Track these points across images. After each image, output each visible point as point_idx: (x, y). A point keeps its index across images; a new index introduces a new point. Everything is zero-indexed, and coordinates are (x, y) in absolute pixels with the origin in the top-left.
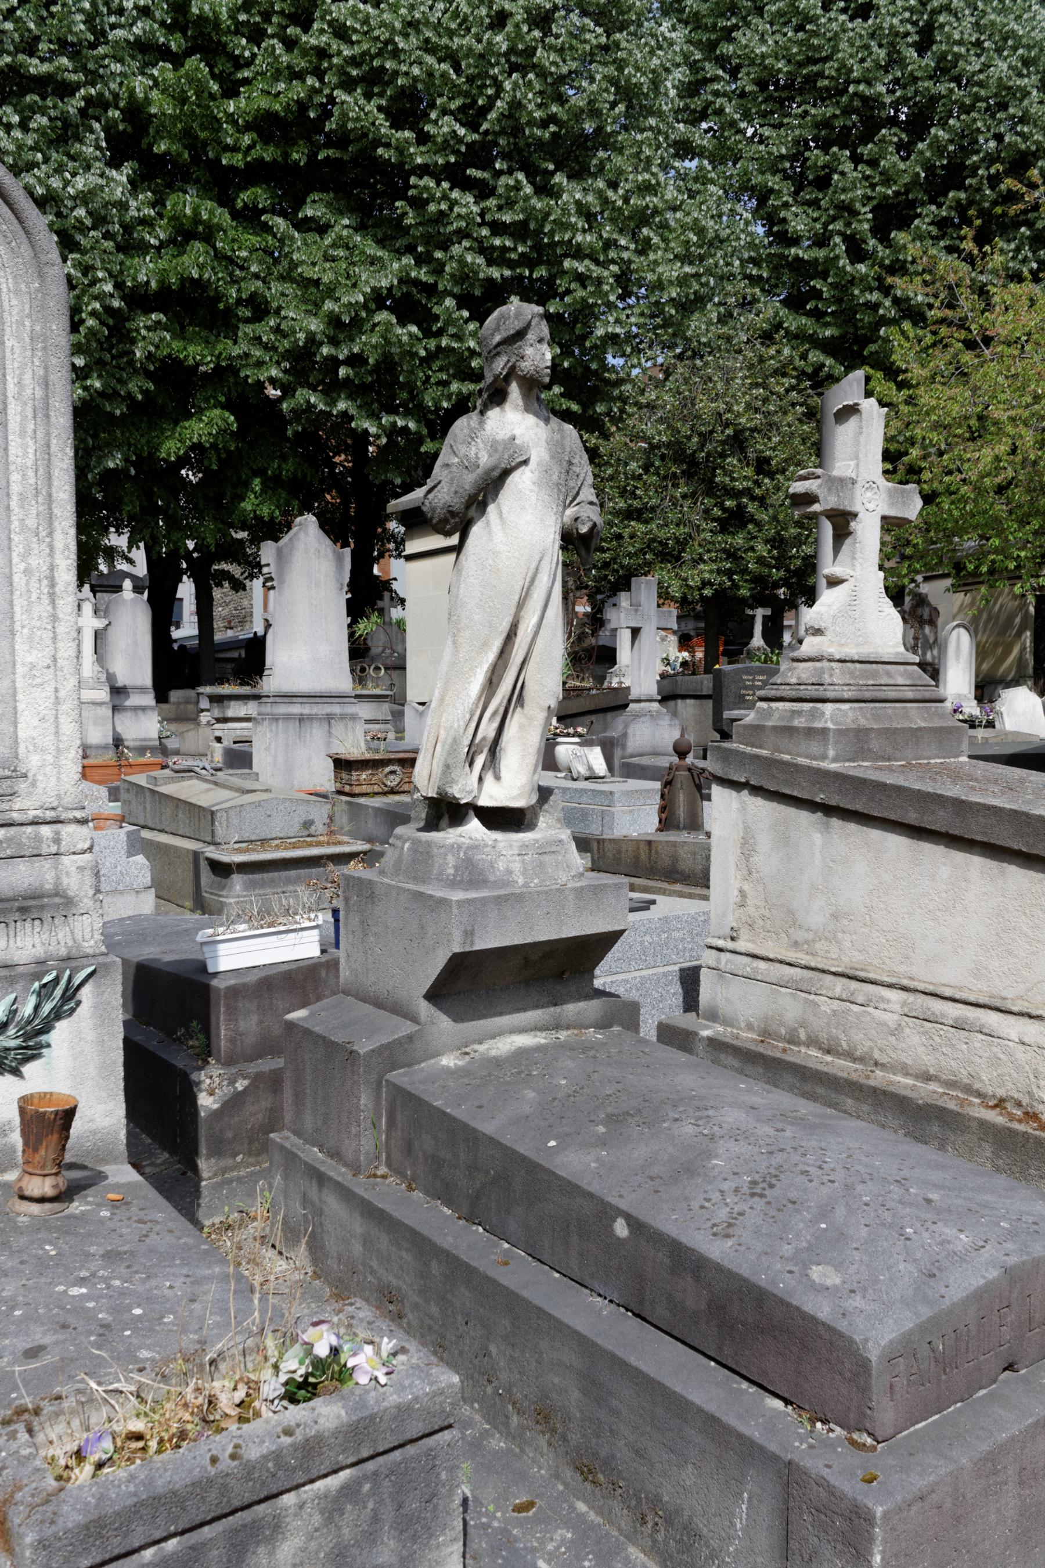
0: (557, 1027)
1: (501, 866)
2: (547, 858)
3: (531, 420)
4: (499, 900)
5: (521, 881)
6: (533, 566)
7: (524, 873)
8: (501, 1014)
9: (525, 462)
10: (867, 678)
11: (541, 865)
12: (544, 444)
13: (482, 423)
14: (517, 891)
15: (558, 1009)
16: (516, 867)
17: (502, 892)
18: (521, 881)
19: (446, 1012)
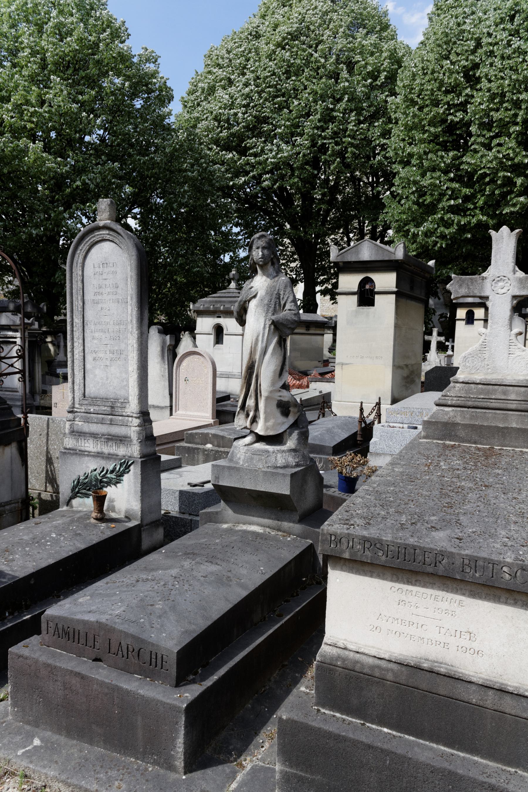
0: (279, 530)
1: (238, 456)
2: (255, 456)
3: (264, 278)
4: (229, 468)
5: (241, 463)
6: (254, 338)
7: (243, 461)
8: (253, 516)
9: (255, 297)
10: (481, 394)
11: (252, 459)
12: (265, 288)
13: (252, 281)
14: (238, 466)
15: (280, 523)
16: (242, 457)
17: (235, 465)
18: (241, 463)
19: (231, 508)
